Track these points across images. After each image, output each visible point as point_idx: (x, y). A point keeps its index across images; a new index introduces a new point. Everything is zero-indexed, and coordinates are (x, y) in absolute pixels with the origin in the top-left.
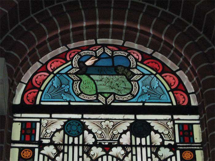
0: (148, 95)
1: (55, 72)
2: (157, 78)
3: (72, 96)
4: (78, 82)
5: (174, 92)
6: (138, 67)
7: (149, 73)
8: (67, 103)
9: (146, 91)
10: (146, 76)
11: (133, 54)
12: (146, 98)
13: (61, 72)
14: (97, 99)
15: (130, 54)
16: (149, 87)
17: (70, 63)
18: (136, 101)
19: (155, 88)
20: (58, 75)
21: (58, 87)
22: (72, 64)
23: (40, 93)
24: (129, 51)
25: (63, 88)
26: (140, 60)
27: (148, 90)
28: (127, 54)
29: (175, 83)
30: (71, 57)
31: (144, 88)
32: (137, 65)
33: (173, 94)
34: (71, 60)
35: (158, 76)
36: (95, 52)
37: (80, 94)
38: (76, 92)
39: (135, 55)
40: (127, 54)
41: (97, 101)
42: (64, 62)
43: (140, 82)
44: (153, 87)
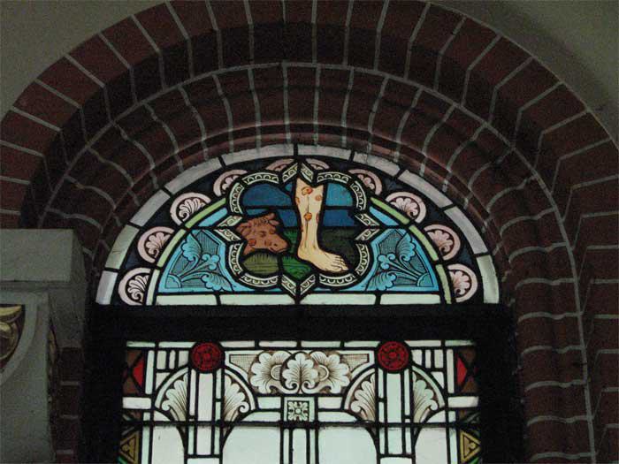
0: (390, 275)
1: (189, 225)
2: (412, 234)
3: (227, 279)
4: (238, 247)
5: (450, 267)
6: (372, 210)
7: (393, 223)
8: (210, 300)
9: (386, 267)
10: (387, 232)
11: (359, 176)
12: (386, 282)
13: (202, 225)
14: (279, 285)
15: (355, 177)
16: (393, 257)
17: (223, 201)
18: (363, 289)
19: (407, 259)
20: (194, 232)
21: (194, 258)
22: (227, 206)
23: (156, 273)
24: (352, 172)
25: (205, 261)
26: (378, 192)
27: (392, 263)
28: (347, 177)
29: (452, 247)
30: (224, 187)
31: (382, 258)
32: (370, 203)
33: (447, 271)
34: (226, 193)
35: (413, 229)
36: (280, 174)
37: (242, 274)
38: (234, 270)
39: (367, 181)
40: (347, 177)
41: (278, 290)
42: (207, 200)
43: (374, 244)
44: (403, 257)
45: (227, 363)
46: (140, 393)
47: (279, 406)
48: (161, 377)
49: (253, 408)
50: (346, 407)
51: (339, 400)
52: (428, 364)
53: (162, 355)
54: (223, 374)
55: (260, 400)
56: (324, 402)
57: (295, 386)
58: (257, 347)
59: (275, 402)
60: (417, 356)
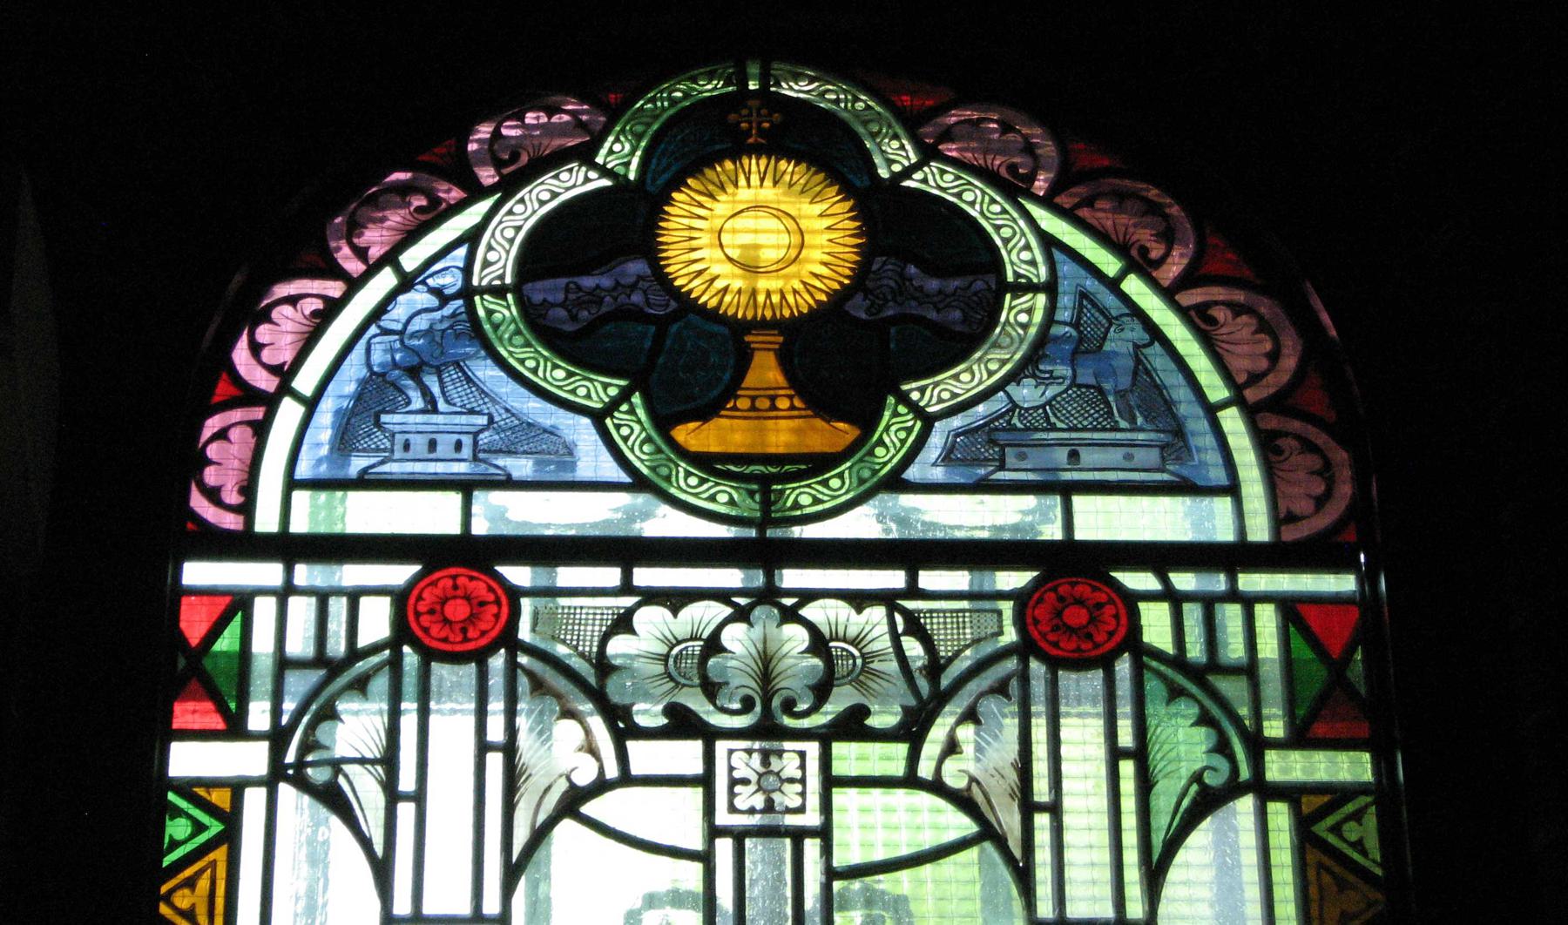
45: (525, 633)
46: (235, 729)
47: (697, 768)
48: (298, 684)
49: (612, 772)
50: (925, 770)
51: (902, 749)
52: (1195, 651)
53: (302, 610)
54: (512, 667)
55: (633, 746)
56: (850, 757)
57: (748, 704)
58: (627, 588)
59: (685, 756)
60: (1156, 625)
